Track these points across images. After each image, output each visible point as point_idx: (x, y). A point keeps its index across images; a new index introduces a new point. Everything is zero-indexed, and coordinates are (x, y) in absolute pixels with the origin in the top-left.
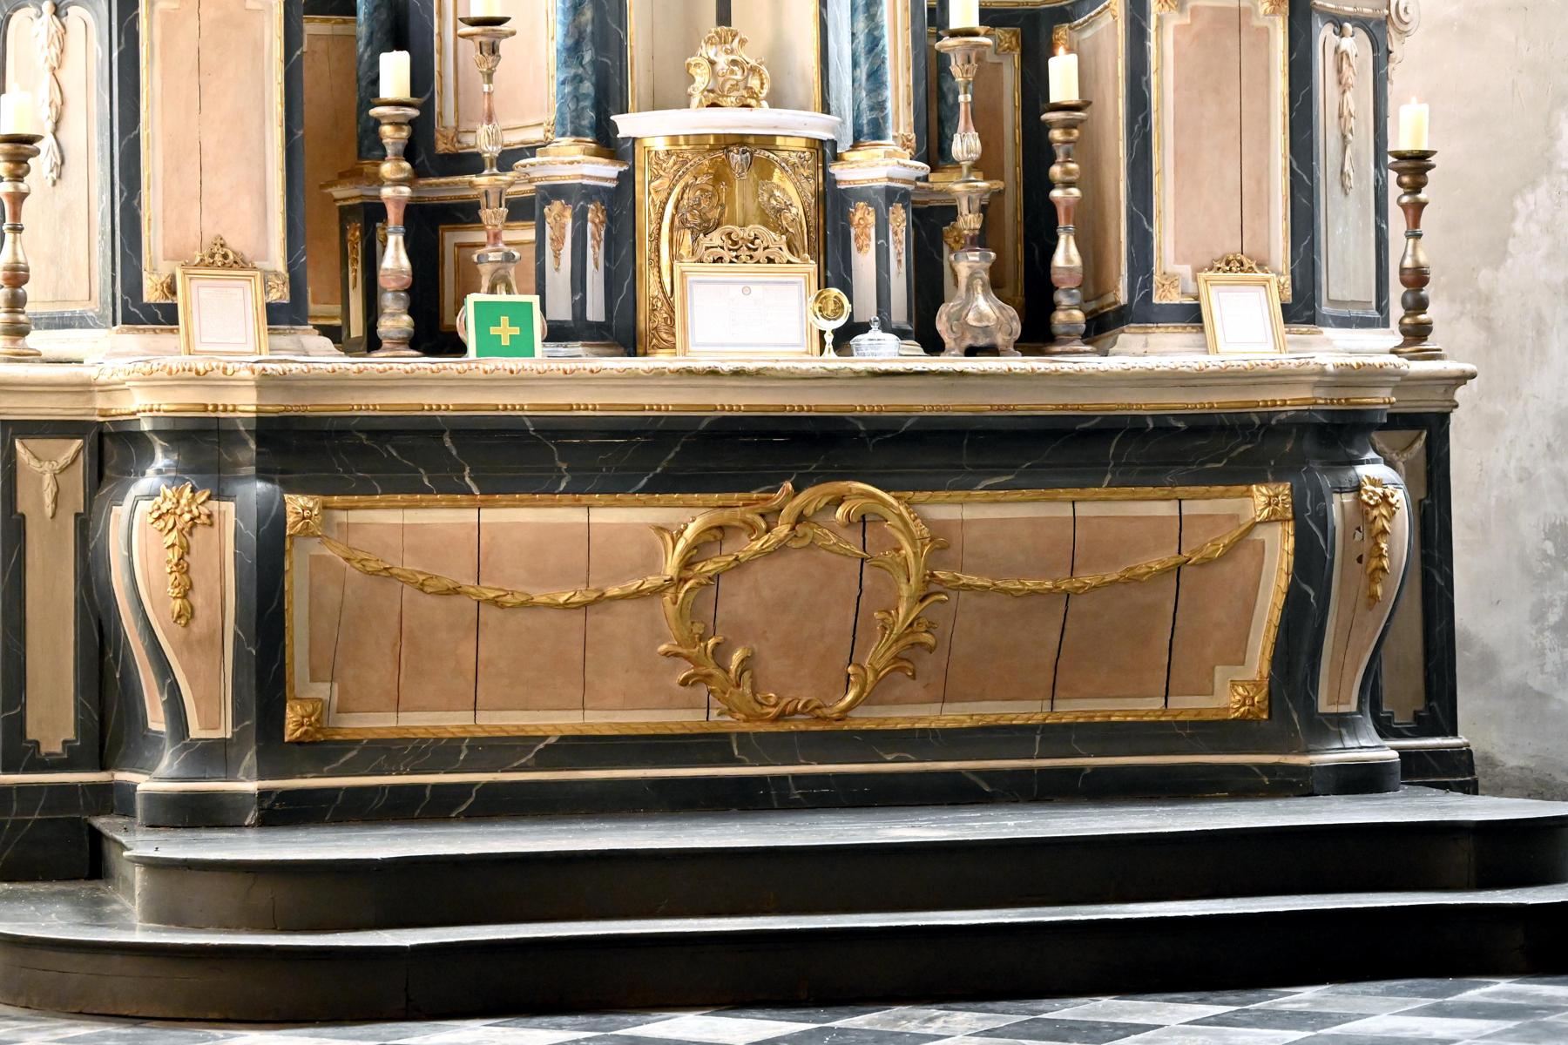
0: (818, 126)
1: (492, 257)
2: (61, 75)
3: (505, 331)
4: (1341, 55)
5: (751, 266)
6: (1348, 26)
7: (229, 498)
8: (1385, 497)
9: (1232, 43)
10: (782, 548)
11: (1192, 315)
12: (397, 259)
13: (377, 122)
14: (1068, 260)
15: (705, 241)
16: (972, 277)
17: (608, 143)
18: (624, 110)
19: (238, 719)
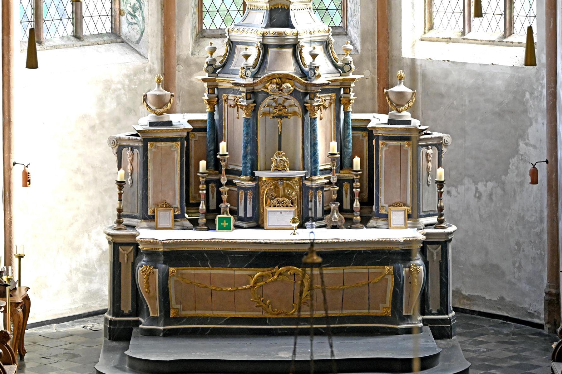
0: (299, 173)
1: (223, 206)
2: (133, 164)
3: (225, 224)
4: (427, 154)
5: (282, 208)
6: (430, 147)
7: (157, 268)
8: (416, 269)
9: (399, 154)
10: (276, 280)
11: (386, 217)
12: (202, 206)
13: (199, 176)
14: (356, 205)
15: (272, 202)
16: (334, 209)
17: (254, 178)
18: (257, 170)
19: (160, 312)
